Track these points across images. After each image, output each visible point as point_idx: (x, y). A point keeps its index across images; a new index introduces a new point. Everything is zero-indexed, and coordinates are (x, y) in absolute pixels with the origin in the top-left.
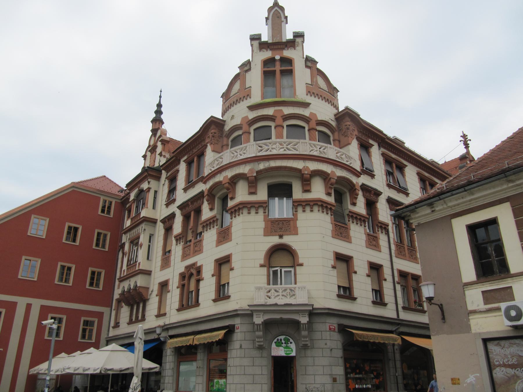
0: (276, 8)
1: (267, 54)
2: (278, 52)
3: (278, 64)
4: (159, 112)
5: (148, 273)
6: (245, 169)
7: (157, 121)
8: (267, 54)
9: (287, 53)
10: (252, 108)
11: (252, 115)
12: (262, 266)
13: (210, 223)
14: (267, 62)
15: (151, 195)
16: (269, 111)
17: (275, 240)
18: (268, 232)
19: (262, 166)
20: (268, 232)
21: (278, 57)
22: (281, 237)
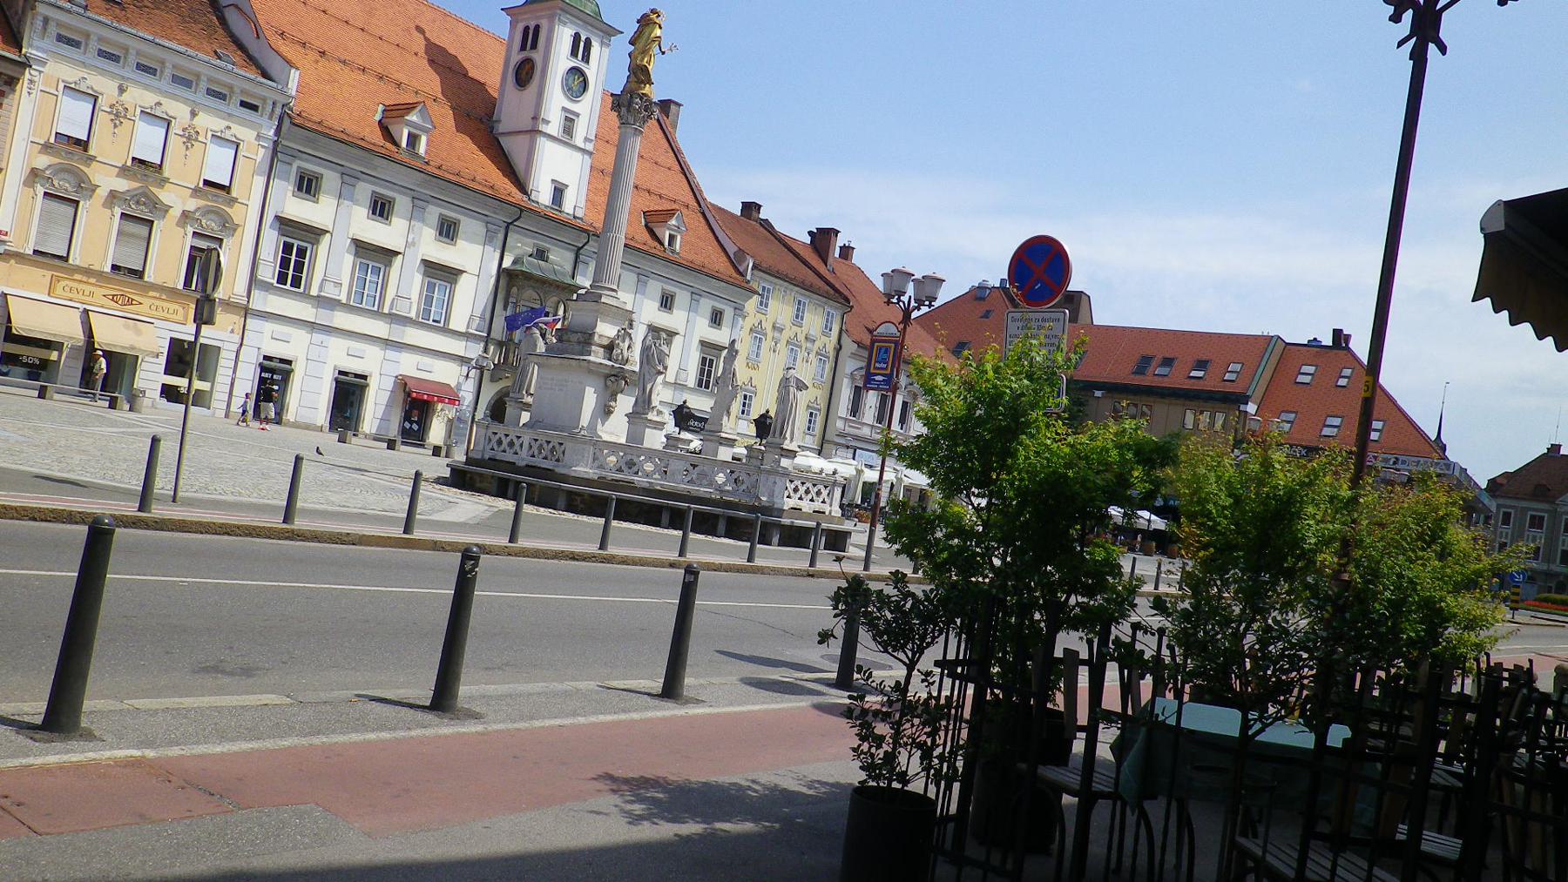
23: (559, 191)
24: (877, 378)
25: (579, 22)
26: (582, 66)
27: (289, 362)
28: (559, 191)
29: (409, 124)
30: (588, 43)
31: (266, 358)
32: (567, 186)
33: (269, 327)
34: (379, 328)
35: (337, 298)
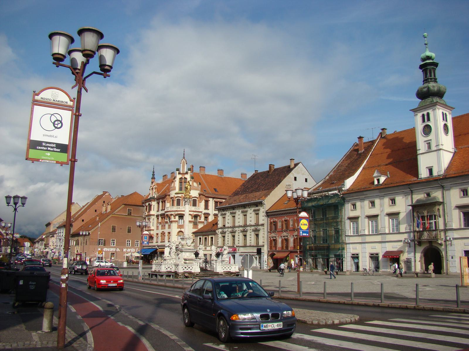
0: (184, 160)
1: (180, 176)
2: (183, 175)
3: (183, 179)
4: (153, 175)
5: (153, 230)
6: (173, 213)
7: (153, 178)
8: (180, 176)
9: (186, 176)
10: (176, 194)
11: (176, 195)
12: (176, 235)
13: (167, 222)
14: (181, 179)
15: (152, 207)
16: (180, 195)
17: (179, 230)
18: (178, 228)
19: (176, 213)
20: (178, 228)
21: (183, 177)
22: (181, 229)
23: (431, 170)
24: (145, 242)
25: (423, 110)
26: (429, 123)
27: (358, 254)
28: (431, 170)
29: (376, 177)
30: (428, 114)
31: (353, 254)
32: (433, 166)
33: (351, 246)
34: (378, 238)
35: (364, 234)
